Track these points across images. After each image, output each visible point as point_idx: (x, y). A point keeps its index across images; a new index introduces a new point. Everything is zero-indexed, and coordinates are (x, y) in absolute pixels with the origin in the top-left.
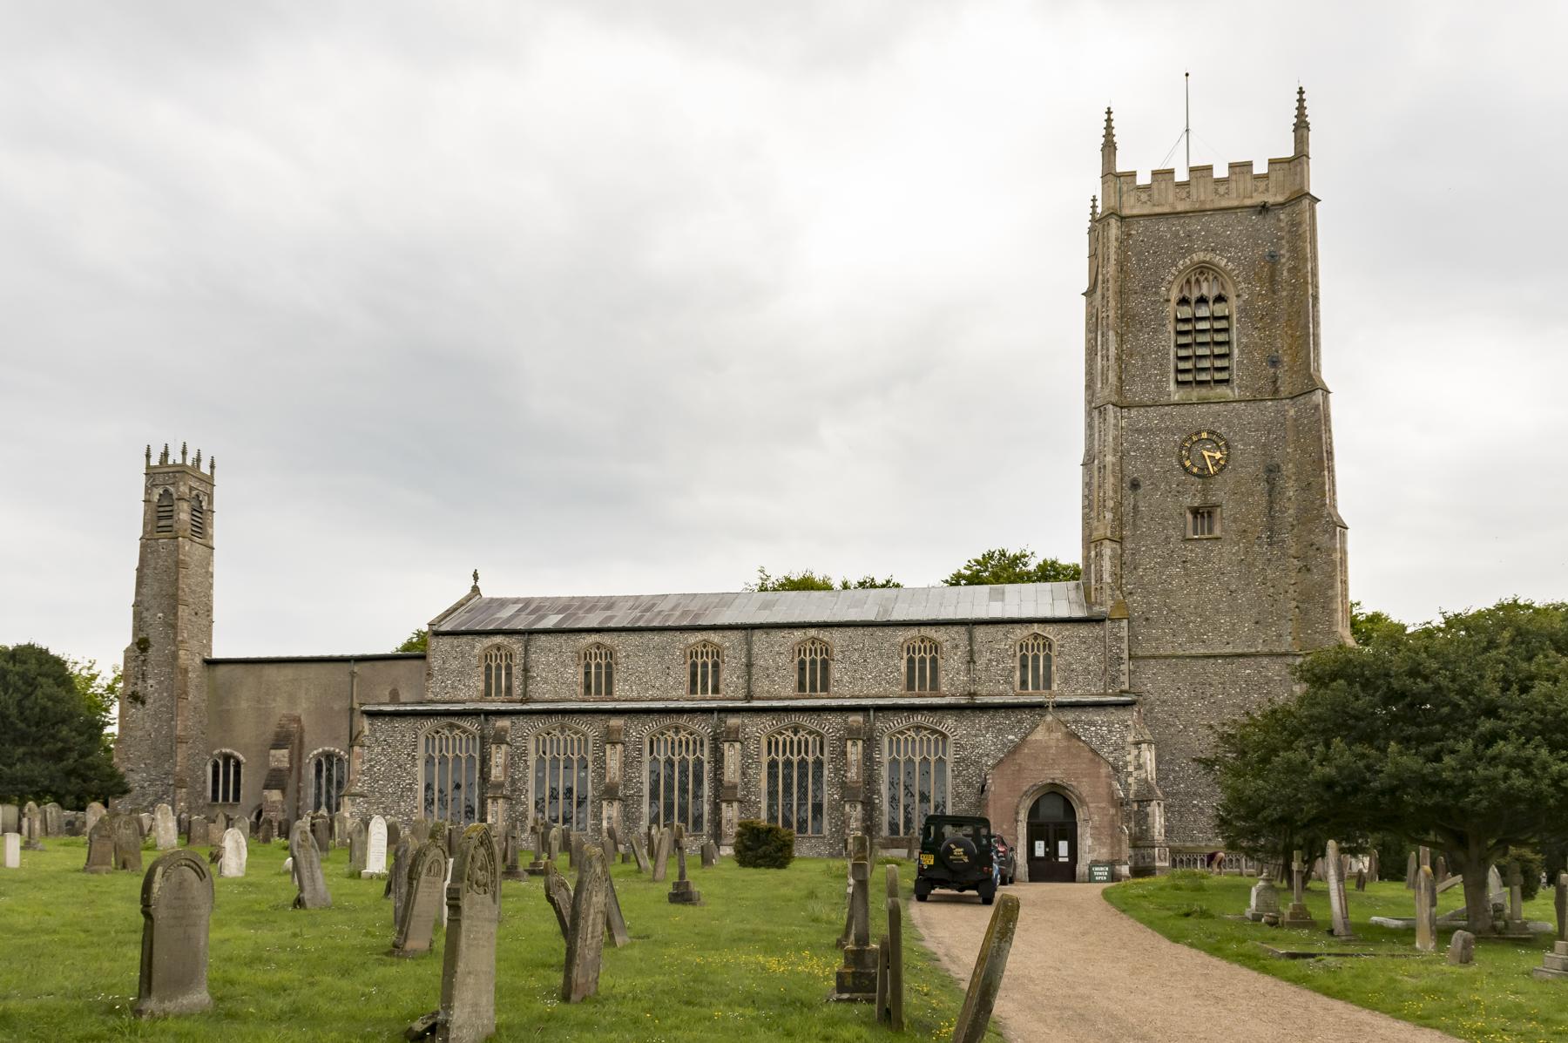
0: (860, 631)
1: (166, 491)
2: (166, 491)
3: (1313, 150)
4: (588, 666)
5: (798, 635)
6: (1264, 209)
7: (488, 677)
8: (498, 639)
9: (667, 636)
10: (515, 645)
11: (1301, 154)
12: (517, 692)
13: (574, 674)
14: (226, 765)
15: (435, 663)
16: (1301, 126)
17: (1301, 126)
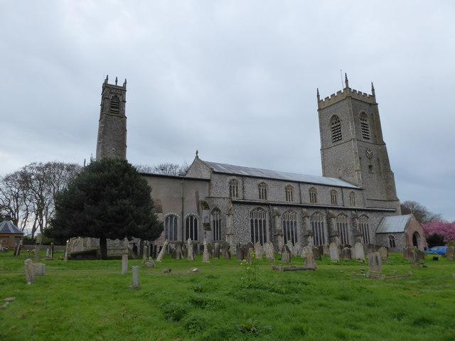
0: (322, 187)
1: (116, 96)
2: (116, 96)
3: (376, 94)
4: (260, 190)
5: (309, 185)
6: (370, 104)
7: (231, 190)
8: (234, 177)
9: (280, 183)
10: (240, 180)
11: (373, 96)
12: (241, 196)
13: (256, 191)
14: (171, 220)
15: (213, 182)
16: (373, 90)
17: (373, 90)
